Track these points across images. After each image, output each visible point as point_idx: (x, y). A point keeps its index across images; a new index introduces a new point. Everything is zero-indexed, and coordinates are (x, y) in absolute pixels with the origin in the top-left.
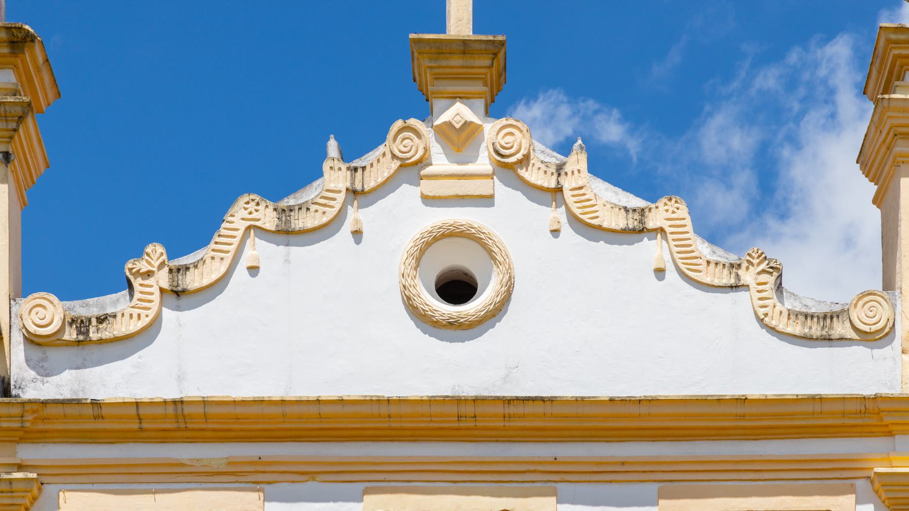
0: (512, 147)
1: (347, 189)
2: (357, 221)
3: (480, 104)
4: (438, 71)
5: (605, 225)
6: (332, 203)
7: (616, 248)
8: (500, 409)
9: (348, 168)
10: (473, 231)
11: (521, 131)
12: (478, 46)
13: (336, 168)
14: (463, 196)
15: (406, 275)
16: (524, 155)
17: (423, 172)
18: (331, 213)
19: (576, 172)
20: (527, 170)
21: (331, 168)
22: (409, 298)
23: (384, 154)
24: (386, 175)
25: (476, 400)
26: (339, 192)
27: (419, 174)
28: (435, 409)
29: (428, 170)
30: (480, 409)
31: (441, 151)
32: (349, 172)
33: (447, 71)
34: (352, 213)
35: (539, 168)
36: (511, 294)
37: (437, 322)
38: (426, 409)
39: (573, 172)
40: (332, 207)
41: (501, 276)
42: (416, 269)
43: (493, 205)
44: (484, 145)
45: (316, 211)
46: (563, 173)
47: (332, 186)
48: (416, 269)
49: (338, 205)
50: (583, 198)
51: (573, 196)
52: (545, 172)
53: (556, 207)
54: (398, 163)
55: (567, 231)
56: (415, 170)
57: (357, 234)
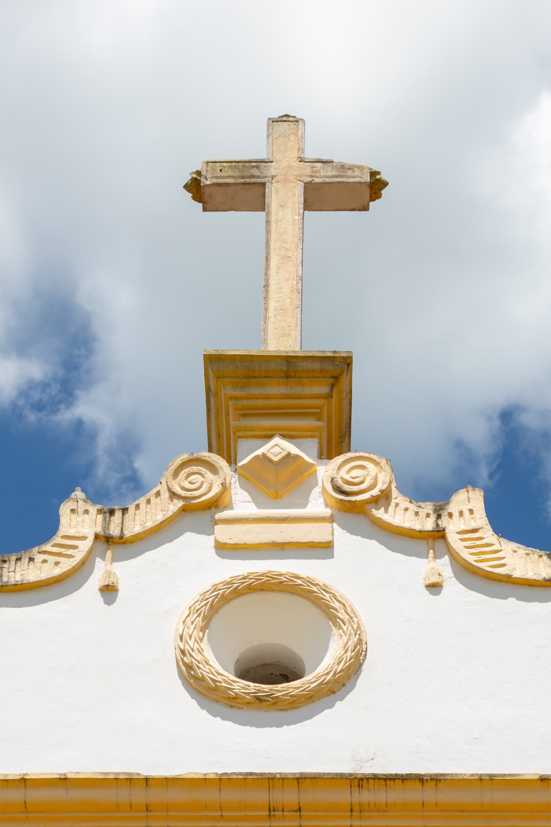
0: (362, 483)
1: (97, 537)
2: (109, 574)
3: (313, 444)
4: (246, 403)
5: (517, 574)
6: (70, 552)
7: (535, 607)
8: (343, 796)
9: (100, 511)
10: (299, 582)
11: (377, 464)
12: (310, 365)
13: (81, 510)
14: (283, 544)
15: (186, 636)
16: (382, 491)
17: (218, 516)
18: (66, 565)
19: (466, 513)
20: (386, 511)
21: (73, 511)
22: (189, 667)
23: (158, 494)
24: (160, 518)
25: (301, 780)
26: (84, 538)
27: (213, 517)
28: (229, 796)
29: (226, 514)
30: (309, 796)
31: (249, 498)
32: (100, 517)
33: (261, 402)
34: (101, 570)
35: (406, 509)
36: (361, 665)
37: (236, 697)
38: (212, 796)
39: (461, 513)
40: (71, 556)
41: (345, 639)
42: (203, 629)
43: (332, 556)
44: (317, 491)
45: (45, 561)
46: (445, 514)
47: (72, 532)
48: (203, 629)
49: (79, 555)
50: (479, 542)
51: (462, 540)
52: (417, 514)
53: (435, 557)
54: (180, 504)
55: (453, 587)
56: (206, 516)
57: (109, 591)
